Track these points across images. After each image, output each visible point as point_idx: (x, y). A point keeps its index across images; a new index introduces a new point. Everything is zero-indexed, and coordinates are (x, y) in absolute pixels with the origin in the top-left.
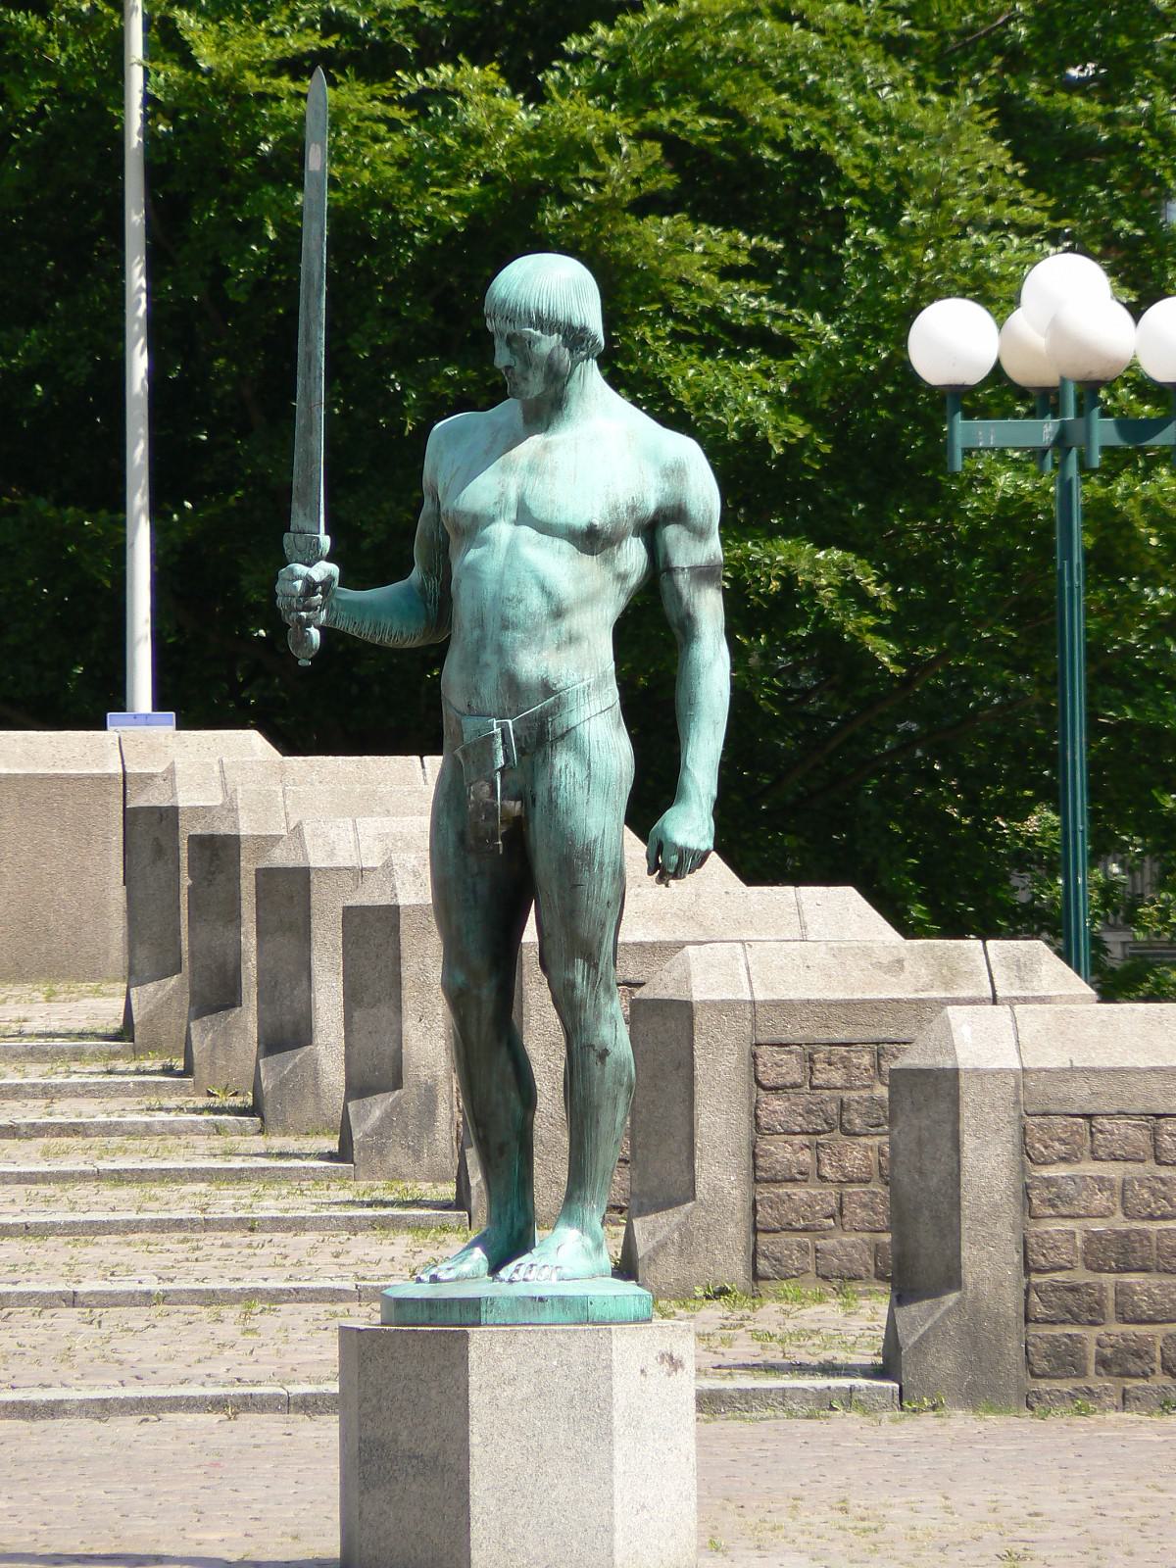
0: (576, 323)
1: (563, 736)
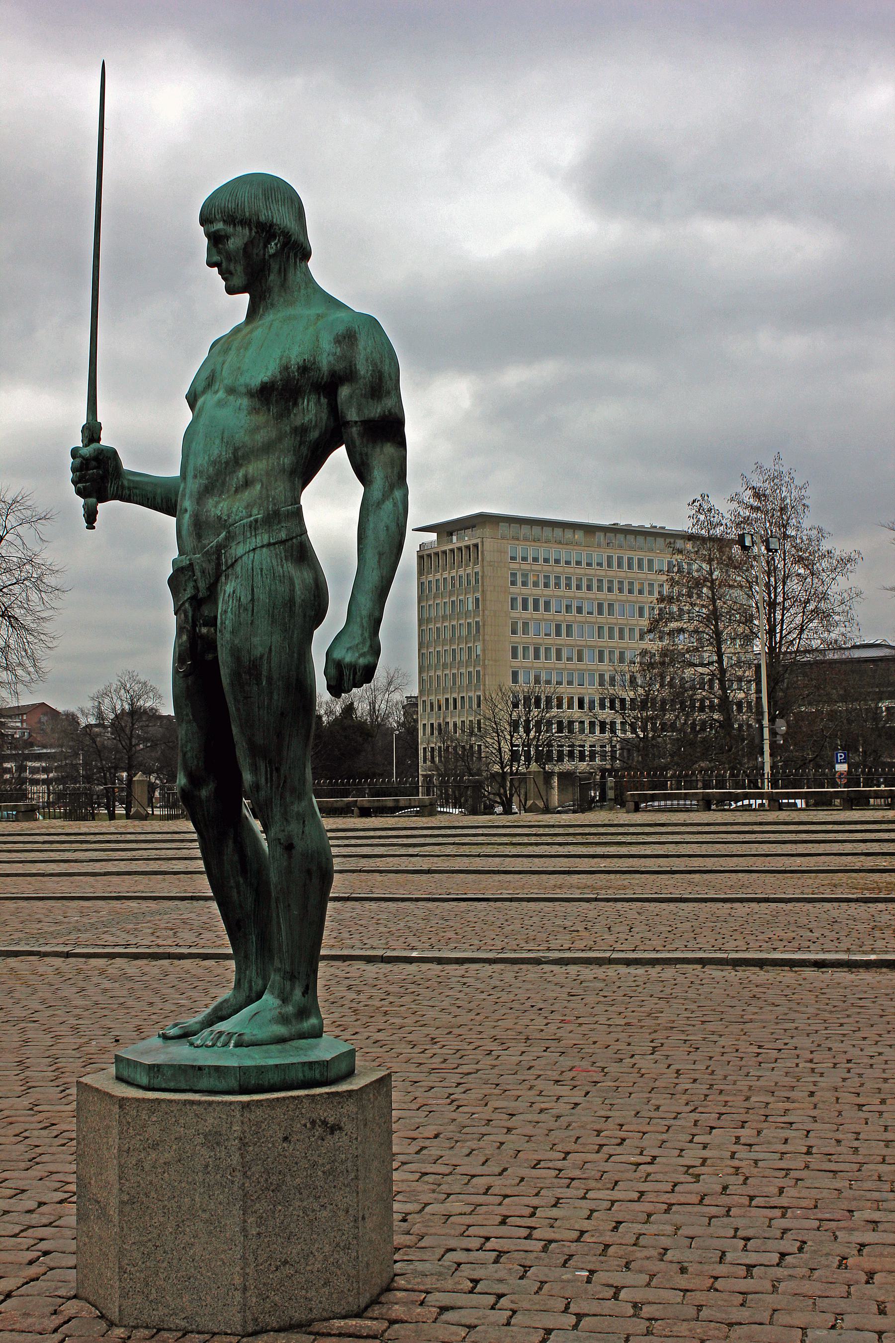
0: (262, 218)
1: (233, 565)
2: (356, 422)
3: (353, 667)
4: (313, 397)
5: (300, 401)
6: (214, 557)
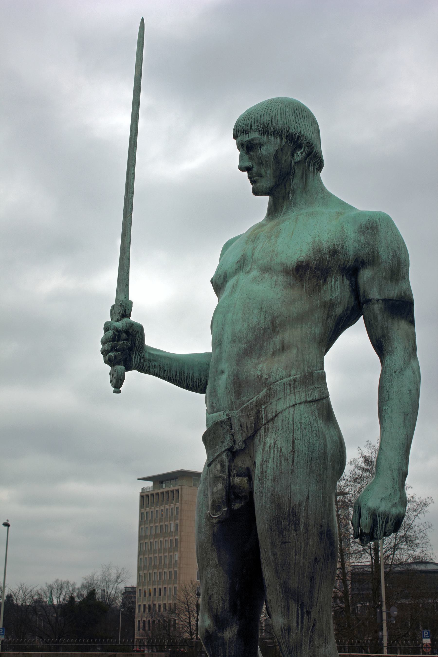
0: (292, 131)
1: (272, 419)
2: (378, 300)
3: (386, 516)
4: (339, 277)
5: (329, 279)
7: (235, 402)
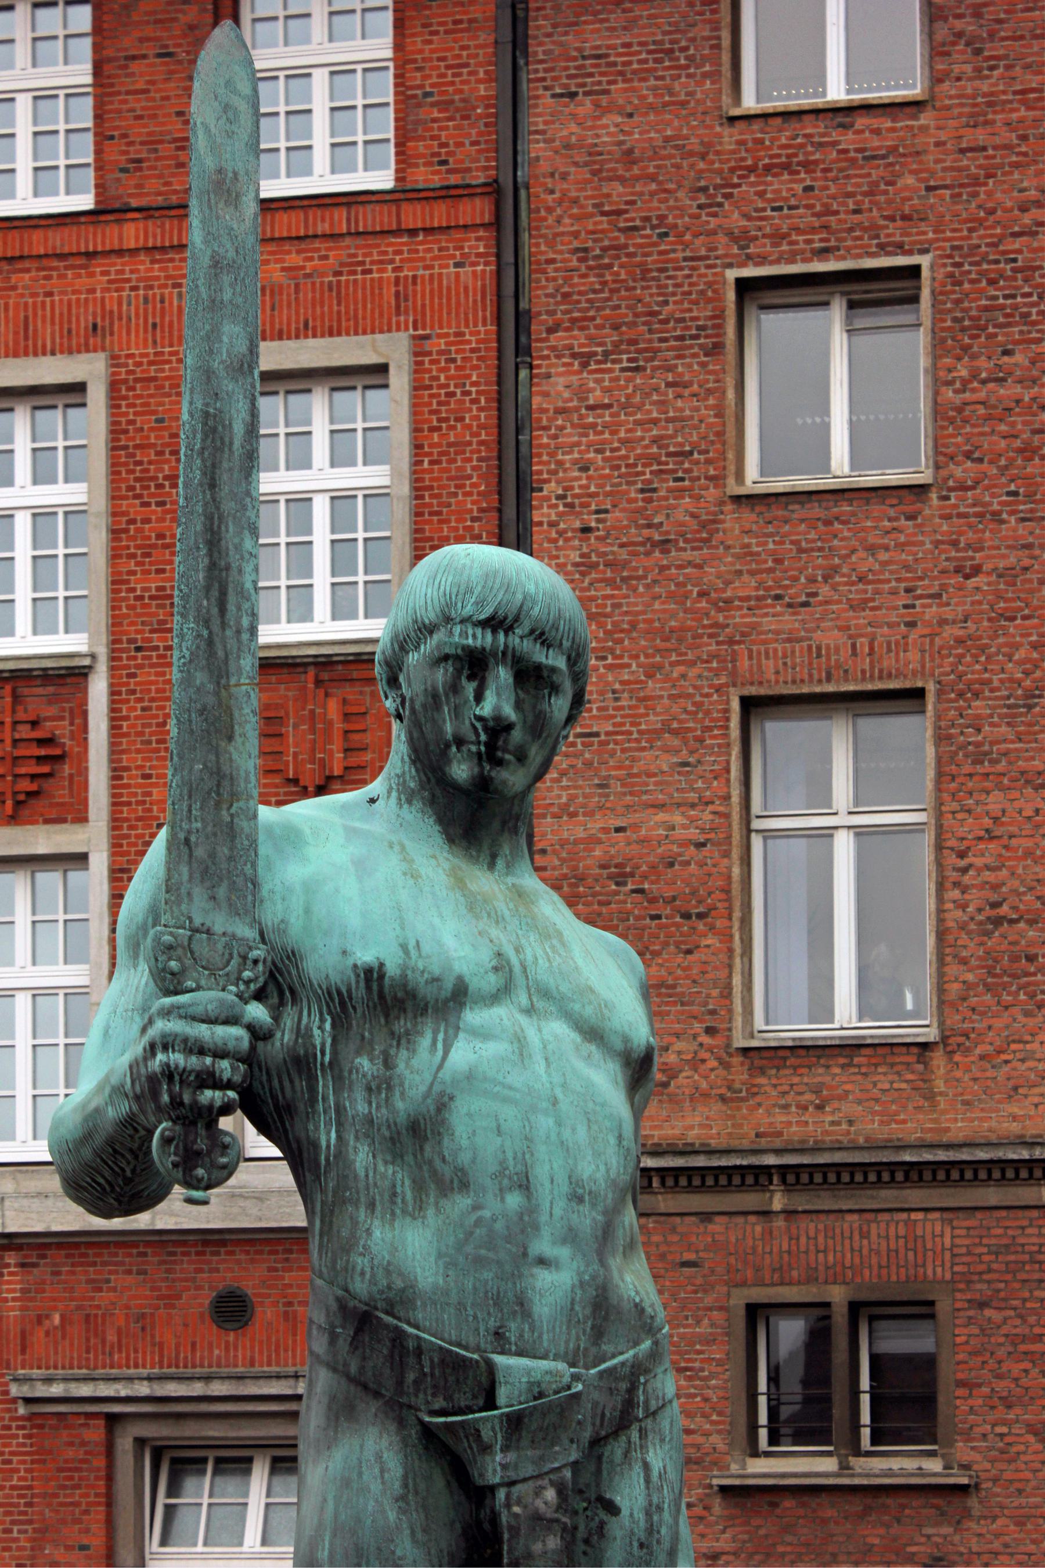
1: (654, 1413)
6: (624, 1386)
7: (586, 1349)
